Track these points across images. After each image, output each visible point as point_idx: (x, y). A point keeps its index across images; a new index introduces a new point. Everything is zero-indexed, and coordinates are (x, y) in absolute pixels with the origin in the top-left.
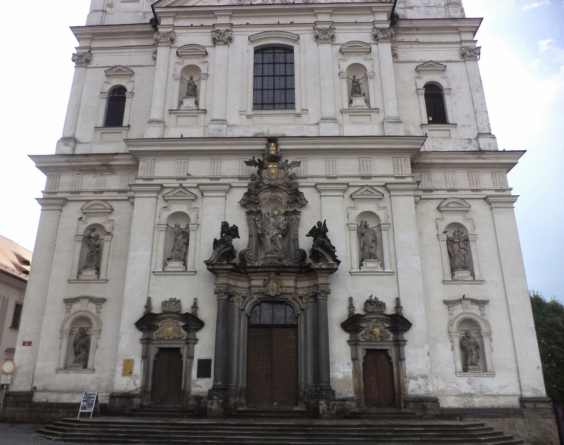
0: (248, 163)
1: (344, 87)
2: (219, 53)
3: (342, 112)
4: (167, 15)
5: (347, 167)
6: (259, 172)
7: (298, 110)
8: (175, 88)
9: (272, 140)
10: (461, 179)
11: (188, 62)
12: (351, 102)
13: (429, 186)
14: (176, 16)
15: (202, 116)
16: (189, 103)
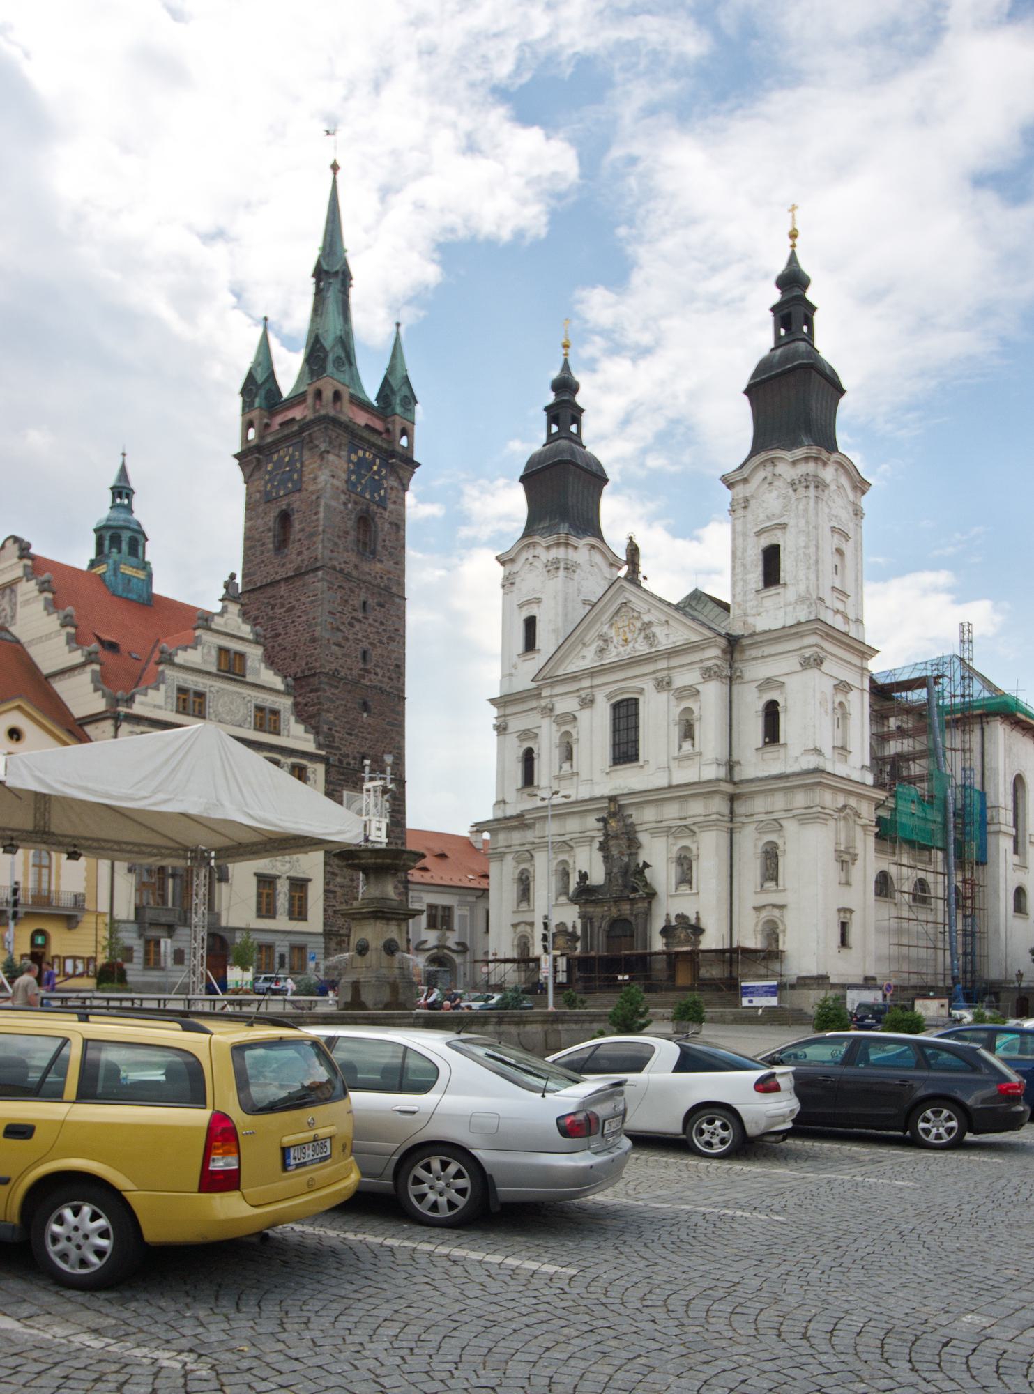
0: (598, 820)
1: (675, 732)
2: (584, 716)
3: (675, 759)
4: (545, 686)
5: (671, 811)
6: (605, 827)
7: (641, 762)
8: (556, 754)
9: (612, 799)
10: (779, 802)
11: (564, 728)
12: (680, 747)
13: (750, 812)
14: (552, 685)
15: (575, 778)
16: (566, 766)
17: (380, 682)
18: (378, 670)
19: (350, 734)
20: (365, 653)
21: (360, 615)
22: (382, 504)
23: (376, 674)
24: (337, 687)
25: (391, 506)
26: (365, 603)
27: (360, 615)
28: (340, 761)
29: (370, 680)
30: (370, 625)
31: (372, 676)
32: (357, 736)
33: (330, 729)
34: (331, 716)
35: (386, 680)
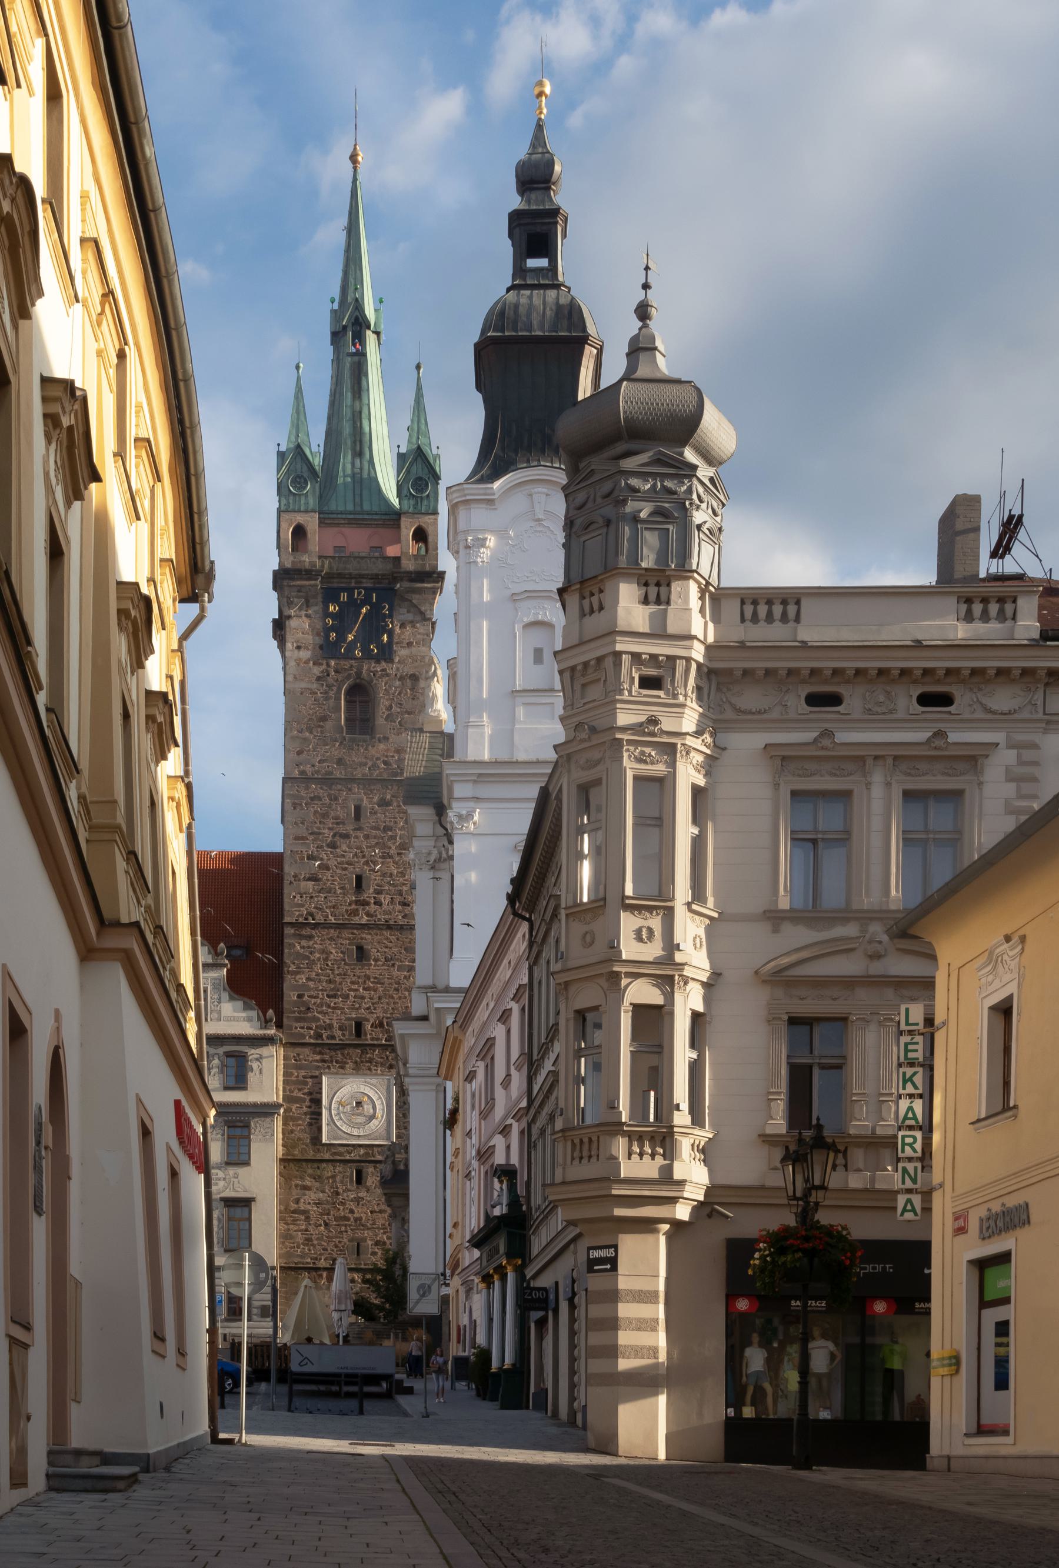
17: (385, 913)
18: (382, 897)
19: (335, 996)
20: (359, 879)
21: (349, 828)
22: (386, 654)
23: (378, 903)
24: (310, 937)
25: (401, 652)
26: (358, 809)
27: (349, 828)
28: (319, 1036)
29: (368, 915)
30: (367, 837)
31: (373, 907)
32: (347, 997)
33: (300, 996)
34: (302, 979)
35: (399, 907)
